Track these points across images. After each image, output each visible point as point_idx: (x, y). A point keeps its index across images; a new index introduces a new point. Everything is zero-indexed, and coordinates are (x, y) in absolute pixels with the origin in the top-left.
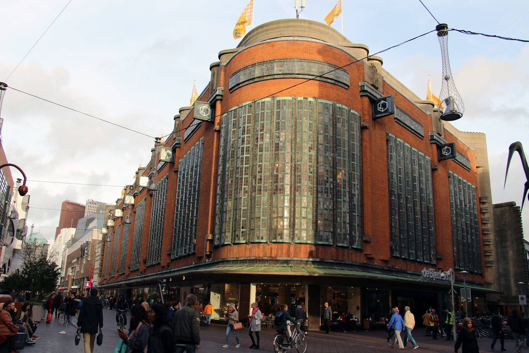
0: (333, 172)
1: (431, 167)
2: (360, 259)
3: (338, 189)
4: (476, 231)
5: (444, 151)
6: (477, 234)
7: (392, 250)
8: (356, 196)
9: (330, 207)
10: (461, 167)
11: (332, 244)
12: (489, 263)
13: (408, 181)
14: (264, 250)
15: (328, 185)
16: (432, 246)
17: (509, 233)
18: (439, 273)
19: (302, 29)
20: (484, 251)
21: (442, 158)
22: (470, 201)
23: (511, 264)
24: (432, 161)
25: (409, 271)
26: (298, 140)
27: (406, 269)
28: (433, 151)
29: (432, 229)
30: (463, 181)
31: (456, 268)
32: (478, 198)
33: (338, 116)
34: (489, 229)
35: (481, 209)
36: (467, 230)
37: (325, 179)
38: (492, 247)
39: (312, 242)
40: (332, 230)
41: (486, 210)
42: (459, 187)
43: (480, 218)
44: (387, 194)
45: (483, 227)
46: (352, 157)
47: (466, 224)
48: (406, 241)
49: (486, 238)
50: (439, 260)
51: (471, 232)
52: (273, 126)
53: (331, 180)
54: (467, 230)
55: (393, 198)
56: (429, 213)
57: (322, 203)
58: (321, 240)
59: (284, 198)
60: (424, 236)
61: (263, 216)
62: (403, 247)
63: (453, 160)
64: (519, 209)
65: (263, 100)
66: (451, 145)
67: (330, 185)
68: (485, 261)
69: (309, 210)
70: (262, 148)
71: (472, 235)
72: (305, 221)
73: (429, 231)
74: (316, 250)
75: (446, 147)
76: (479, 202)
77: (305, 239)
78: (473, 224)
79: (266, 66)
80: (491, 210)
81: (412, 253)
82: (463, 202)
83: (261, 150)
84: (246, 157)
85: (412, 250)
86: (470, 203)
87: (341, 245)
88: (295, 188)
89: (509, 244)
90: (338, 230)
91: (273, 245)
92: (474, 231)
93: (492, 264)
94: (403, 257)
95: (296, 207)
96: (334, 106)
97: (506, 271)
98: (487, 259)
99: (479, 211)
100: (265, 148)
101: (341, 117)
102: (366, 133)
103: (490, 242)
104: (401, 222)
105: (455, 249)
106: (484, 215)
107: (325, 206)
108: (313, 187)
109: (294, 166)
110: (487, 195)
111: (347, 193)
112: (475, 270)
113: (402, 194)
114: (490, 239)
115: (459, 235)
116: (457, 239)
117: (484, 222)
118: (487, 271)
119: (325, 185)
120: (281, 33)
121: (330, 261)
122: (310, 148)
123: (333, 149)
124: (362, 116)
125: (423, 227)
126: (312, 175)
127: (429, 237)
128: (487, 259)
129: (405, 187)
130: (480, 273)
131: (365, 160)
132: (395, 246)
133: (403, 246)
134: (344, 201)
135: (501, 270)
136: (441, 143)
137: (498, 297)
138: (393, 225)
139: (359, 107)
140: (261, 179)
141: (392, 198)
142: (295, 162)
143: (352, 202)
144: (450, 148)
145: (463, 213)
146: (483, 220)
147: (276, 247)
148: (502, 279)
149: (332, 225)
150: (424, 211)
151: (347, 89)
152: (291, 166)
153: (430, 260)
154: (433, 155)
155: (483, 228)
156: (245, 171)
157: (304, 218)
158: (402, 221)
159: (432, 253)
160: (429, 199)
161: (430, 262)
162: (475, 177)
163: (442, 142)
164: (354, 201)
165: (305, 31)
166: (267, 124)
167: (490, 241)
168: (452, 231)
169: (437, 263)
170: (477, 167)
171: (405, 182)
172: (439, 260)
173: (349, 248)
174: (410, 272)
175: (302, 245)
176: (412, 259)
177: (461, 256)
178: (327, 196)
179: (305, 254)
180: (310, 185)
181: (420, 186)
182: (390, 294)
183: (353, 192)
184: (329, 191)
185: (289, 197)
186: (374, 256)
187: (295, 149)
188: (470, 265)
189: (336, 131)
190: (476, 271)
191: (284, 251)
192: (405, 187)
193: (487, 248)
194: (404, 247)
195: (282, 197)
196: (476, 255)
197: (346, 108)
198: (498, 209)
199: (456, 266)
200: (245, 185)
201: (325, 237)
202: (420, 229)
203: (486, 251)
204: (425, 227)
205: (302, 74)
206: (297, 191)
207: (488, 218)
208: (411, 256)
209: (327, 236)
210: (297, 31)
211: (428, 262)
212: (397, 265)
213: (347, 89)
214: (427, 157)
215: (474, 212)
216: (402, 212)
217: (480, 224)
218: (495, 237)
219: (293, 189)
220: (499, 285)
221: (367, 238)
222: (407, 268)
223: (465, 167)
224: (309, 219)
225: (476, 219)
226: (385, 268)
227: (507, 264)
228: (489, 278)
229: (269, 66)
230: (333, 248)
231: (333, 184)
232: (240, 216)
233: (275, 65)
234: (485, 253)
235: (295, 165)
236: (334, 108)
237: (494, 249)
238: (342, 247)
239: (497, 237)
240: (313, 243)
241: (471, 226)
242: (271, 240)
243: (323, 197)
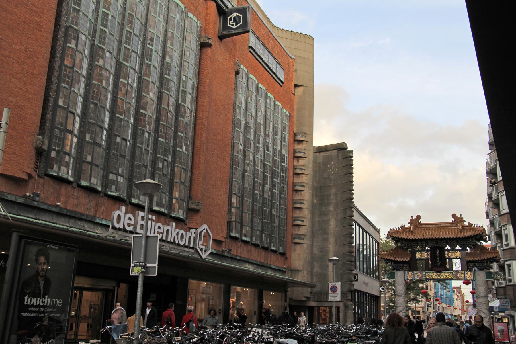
1: (199, 38)
4: (281, 182)
5: (231, 20)
6: (283, 187)
10: (266, 72)
12: (299, 238)
13: (131, 33)
16: (178, 181)
17: (333, 191)
18: (169, 227)
20: (293, 217)
21: (226, 33)
22: (277, 132)
23: (332, 240)
24: (202, 30)
25: (102, 219)
27: (92, 214)
28: (208, 12)
29: (181, 148)
30: (266, 94)
31: (233, 234)
32: (292, 134)
34: (304, 183)
35: (295, 152)
36: (264, 178)
38: (306, 213)
41: (302, 152)
42: (257, 101)
43: (291, 166)
45: (297, 180)
47: (264, 165)
48: (100, 152)
49: (297, 197)
50: (192, 211)
51: (272, 181)
54: (264, 178)
55: (73, 45)
56: (180, 118)
60: (159, 157)
62: (88, 163)
63: (250, 51)
64: (351, 155)
66: (243, 11)
68: (292, 235)
71: (273, 185)
73: (174, 152)
75: (235, 14)
76: (292, 140)
78: (277, 169)
80: (311, 155)
81: (116, 183)
82: (262, 127)
85: (118, 175)
86: (275, 133)
89: (331, 208)
92: (278, 181)
93: (303, 239)
94: (84, 183)
97: (324, 251)
98: (296, 231)
99: (292, 154)
103: (304, 204)
104: (92, 106)
105: (234, 200)
106: (298, 161)
110: (306, 130)
112: (272, 245)
113: (104, 49)
114: (304, 200)
115: (246, 179)
116: (243, 188)
117: (298, 171)
118: (295, 250)
125: (160, 139)
128: (296, 231)
129: (120, 42)
130: (281, 251)
132: (58, 152)
133: (89, 159)
135: (316, 251)
136: (227, 7)
137: (306, 292)
138: (61, 103)
141: (68, 45)
144: (241, 16)
145: (260, 146)
146: (296, 169)
148: (315, 264)
150: (166, 107)
153: (170, 206)
154: (206, 19)
155: (295, 181)
158: (96, 104)
159: (177, 196)
160: (184, 92)
161: (169, 213)
162: (291, 101)
163: (230, 6)
167: (304, 202)
168: (232, 169)
169: (187, 218)
170: (296, 86)
171: (121, 34)
172: (192, 211)
176: (114, 194)
177: (247, 218)
181: (163, 58)
188: (264, 235)
190: (274, 246)
192: (120, 42)
193: (297, 214)
194: (91, 163)
196: (277, 221)
198: (322, 154)
199: (234, 231)
203: (295, 217)
204: (163, 140)
207: (304, 166)
208: (113, 187)
212: (62, 199)
214: (191, 15)
215: (281, 149)
216: (99, 85)
217: (292, 174)
218: (313, 198)
220: (311, 273)
222: (96, 211)
223: (273, 75)
225: (283, 162)
226: (9, 197)
227: (326, 240)
228: (296, 261)
234: (295, 220)
237: (309, 216)
239: (314, 197)
241: (273, 172)
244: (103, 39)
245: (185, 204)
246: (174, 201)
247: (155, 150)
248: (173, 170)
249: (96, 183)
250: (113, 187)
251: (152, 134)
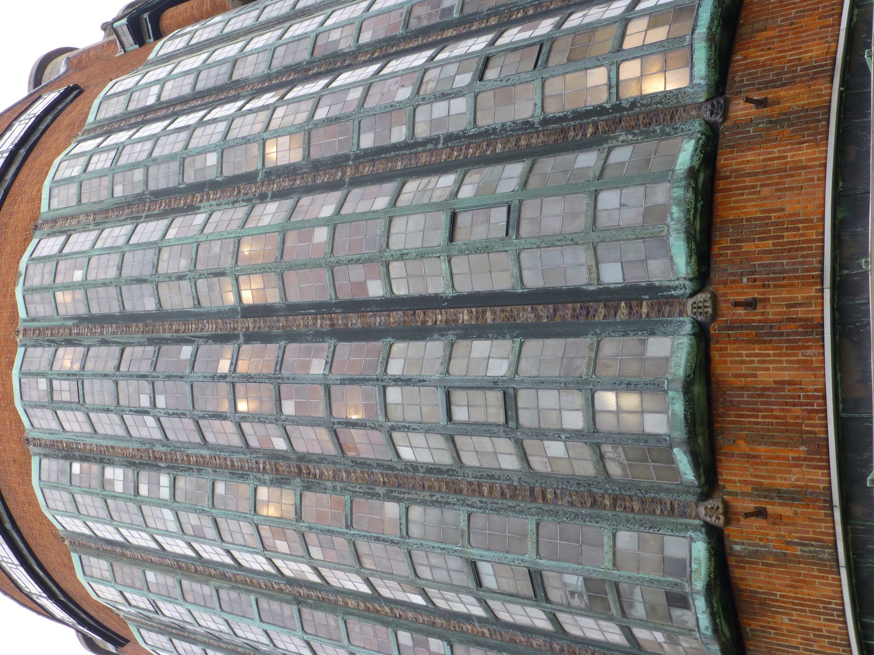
14: (784, 559)
39: (690, 137)
52: (113, 447)
59: (399, 381)
72: (529, 210)
77: (661, 193)
95: (450, 293)
109: (250, 323)
147: (743, 447)
151: (81, 92)
152: (250, 338)
157: (513, 223)
179: (788, 182)
191: (767, 376)
206: (362, 286)
219: (355, 321)
224: (524, 184)
240: (697, 126)
242: (687, 488)
243: (409, 109)
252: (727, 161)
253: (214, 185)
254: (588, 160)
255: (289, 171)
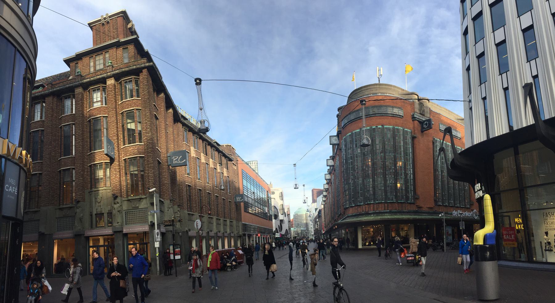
0: (394, 163)
2: (413, 208)
3: (397, 172)
7: (436, 201)
8: (409, 174)
9: (393, 182)
11: (395, 202)
15: (391, 171)
19: (375, 89)
26: (374, 149)
33: (396, 133)
37: (390, 167)
40: (395, 194)
44: (432, 171)
46: (406, 154)
48: (447, 196)
53: (393, 167)
55: (437, 173)
57: (388, 180)
58: (389, 201)
59: (369, 180)
61: (360, 191)
65: (355, 131)
67: (393, 170)
69: (382, 185)
70: (357, 156)
72: (380, 190)
74: (387, 206)
79: (356, 113)
83: (357, 157)
84: (351, 162)
87: (400, 202)
88: (374, 174)
90: (398, 194)
91: (366, 206)
94: (444, 205)
96: (394, 128)
100: (359, 156)
101: (397, 133)
102: (416, 140)
107: (390, 182)
108: (384, 172)
109: (373, 163)
111: (403, 174)
113: (443, 171)
119: (390, 170)
120: (364, 93)
121: (394, 211)
122: (380, 152)
123: (394, 151)
124: (413, 131)
126: (382, 166)
127: (464, 192)
131: (415, 154)
133: (444, 199)
134: (401, 178)
139: (411, 126)
140: (358, 172)
142: (374, 161)
143: (406, 178)
149: (394, 191)
151: (402, 118)
153: (465, 205)
156: (351, 169)
164: (408, 177)
165: (377, 90)
166: (358, 143)
173: (405, 203)
174: (450, 213)
175: (380, 204)
178: (391, 176)
180: (382, 171)
182: (435, 227)
183: (407, 172)
184: (392, 174)
185: (372, 180)
186: (423, 206)
187: (373, 154)
189: (395, 141)
194: (445, 199)
195: (368, 180)
197: (402, 128)
200: (352, 176)
201: (391, 198)
202: (457, 189)
205: (374, 114)
208: (451, 204)
209: (392, 198)
210: (372, 90)
211: (464, 207)
212: (441, 209)
213: (402, 118)
221: (416, 197)
226: (431, 212)
229: (357, 113)
230: (396, 205)
231: (394, 169)
232: (351, 192)
233: (360, 112)
235: (374, 162)
236: (394, 129)
238: (401, 203)
244: (443, 168)
245: (469, 203)
246: (466, 203)
247: (459, 191)
248: (464, 195)
249: (447, 204)
250: (451, 204)
251: (458, 187)
252: (383, 204)
253: (385, 154)
254: (384, 194)
255: (385, 165)
